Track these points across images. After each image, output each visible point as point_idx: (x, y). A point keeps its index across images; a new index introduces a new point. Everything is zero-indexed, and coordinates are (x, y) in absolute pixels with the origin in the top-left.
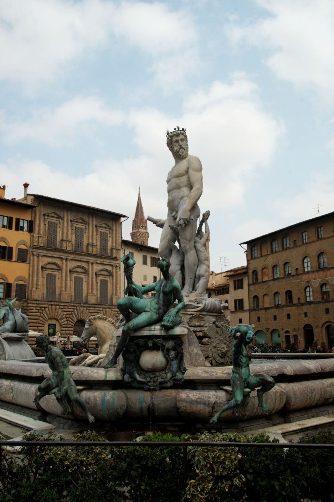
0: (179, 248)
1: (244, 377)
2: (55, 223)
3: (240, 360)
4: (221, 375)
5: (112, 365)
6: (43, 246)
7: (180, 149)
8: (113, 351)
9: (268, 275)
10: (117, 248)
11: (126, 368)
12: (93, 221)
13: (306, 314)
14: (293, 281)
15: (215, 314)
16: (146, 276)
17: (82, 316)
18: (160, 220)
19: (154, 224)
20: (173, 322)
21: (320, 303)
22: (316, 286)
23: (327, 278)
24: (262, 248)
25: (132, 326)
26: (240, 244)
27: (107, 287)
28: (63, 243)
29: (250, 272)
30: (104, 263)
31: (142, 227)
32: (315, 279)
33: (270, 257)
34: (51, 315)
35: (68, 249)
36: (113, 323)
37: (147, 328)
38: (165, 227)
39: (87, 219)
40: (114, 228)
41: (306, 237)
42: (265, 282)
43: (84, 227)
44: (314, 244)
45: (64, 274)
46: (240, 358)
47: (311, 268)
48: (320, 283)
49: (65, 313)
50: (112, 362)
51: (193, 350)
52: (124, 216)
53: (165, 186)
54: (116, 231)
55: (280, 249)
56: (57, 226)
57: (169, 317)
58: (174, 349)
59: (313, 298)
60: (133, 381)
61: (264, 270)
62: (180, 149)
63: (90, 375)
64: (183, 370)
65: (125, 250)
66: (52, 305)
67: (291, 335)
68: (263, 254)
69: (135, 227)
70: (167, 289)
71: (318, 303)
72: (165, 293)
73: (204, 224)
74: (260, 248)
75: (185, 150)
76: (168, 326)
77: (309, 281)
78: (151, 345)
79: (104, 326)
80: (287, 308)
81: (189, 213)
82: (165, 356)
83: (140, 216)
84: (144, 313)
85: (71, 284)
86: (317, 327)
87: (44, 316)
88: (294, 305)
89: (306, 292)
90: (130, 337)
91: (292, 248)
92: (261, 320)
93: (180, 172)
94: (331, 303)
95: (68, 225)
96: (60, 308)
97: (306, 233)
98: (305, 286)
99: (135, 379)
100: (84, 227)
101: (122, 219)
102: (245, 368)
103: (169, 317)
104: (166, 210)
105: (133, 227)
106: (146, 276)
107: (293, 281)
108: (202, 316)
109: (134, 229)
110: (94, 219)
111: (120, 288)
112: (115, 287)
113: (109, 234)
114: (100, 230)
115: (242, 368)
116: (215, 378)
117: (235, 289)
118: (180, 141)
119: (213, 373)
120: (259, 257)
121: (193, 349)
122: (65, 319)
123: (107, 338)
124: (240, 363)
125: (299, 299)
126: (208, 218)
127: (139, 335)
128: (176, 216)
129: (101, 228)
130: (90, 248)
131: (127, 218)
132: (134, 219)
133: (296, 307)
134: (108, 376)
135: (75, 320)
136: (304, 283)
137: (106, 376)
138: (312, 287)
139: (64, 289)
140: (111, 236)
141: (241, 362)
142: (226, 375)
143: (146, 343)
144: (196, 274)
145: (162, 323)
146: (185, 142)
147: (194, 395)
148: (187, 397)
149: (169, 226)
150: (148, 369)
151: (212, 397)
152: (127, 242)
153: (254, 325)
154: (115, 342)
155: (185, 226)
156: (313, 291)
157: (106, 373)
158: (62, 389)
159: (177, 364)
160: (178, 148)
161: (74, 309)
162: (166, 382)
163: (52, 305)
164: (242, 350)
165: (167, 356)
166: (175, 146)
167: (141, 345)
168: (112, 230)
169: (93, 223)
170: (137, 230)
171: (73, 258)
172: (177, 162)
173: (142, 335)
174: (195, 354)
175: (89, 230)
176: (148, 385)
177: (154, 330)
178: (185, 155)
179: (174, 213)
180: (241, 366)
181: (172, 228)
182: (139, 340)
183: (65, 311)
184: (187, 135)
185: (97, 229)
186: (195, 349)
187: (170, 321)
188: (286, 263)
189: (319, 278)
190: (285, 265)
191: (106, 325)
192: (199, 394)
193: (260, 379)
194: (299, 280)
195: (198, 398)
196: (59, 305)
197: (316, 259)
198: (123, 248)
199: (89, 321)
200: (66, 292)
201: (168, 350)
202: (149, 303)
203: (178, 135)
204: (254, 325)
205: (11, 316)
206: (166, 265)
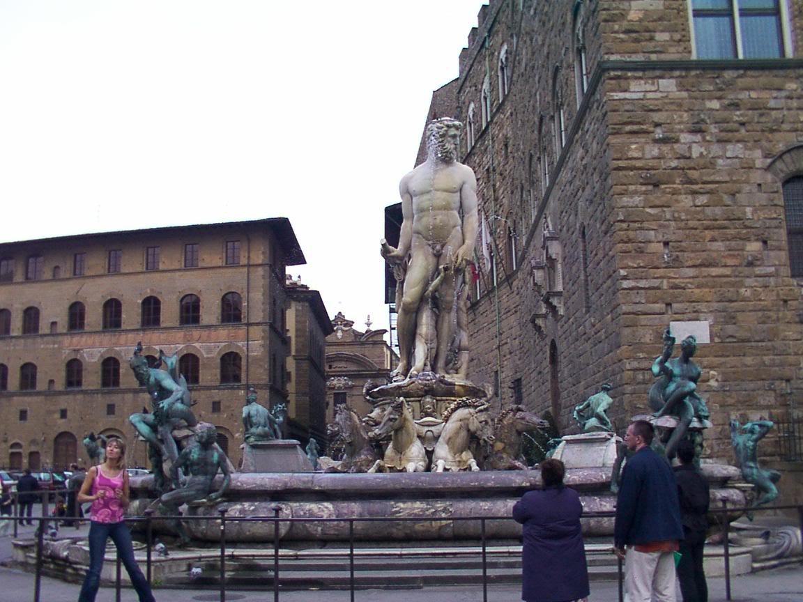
13: (64, 414)
14: (42, 346)
21: (97, 394)
22: (93, 361)
23: (117, 349)
32: (92, 347)
44: (99, 281)
48: (102, 356)
55: (19, 277)
67: (25, 451)
71: (94, 394)
77: (78, 350)
80: (21, 398)
88: (39, 394)
91: (46, 281)
94: (120, 396)
107: (42, 346)
125: (51, 382)
133: (43, 397)
136: (67, 351)
166: (449, 142)
189: (101, 346)
193: (772, 474)
194: (56, 346)
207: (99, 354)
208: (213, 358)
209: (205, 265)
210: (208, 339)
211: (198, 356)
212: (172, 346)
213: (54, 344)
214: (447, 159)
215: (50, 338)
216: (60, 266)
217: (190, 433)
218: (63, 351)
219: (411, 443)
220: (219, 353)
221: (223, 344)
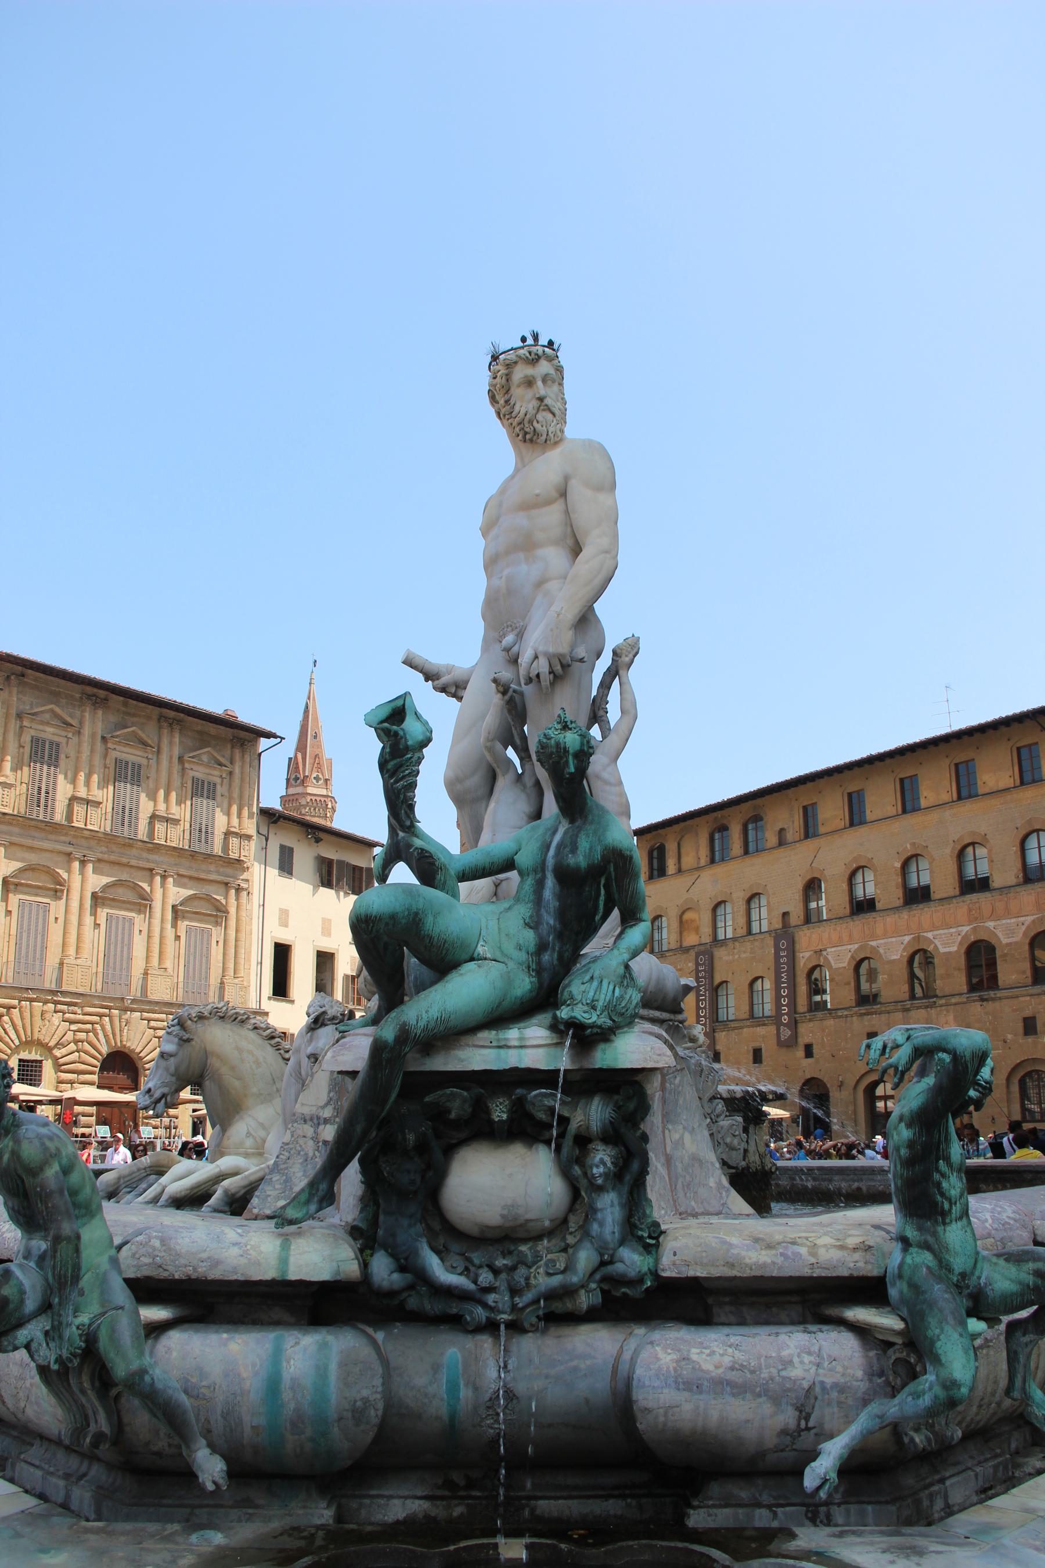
0: (520, 771)
1: (959, 1263)
2: (51, 743)
3: (938, 1185)
4: (835, 1255)
5: (313, 1207)
6: (11, 812)
8: (311, 1143)
10: (243, 832)
11: (374, 1223)
12: (171, 743)
15: (657, 1014)
16: (330, 920)
17: (125, 1039)
18: (450, 669)
19: (427, 680)
20: (610, 1008)
23: (873, 943)
24: (683, 851)
25: (421, 1024)
27: (209, 949)
28: (76, 808)
30: (203, 876)
31: (317, 779)
33: (706, 875)
34: (29, 1034)
35: (89, 827)
36: (273, 1038)
37: (486, 1036)
38: (467, 694)
39: (151, 739)
40: (237, 770)
42: (686, 950)
43: (144, 762)
45: (75, 904)
46: (936, 1176)
48: (852, 957)
49: (74, 1027)
50: (311, 1196)
51: (679, 1143)
52: (269, 735)
53: (476, 547)
54: (242, 780)
56: (57, 752)
57: (595, 983)
58: (611, 1136)
60: (411, 1287)
61: (688, 916)
63: (204, 1255)
64: (646, 1235)
65: (267, 840)
66: (31, 1000)
68: (684, 867)
69: (297, 779)
70: (580, 859)
72: (566, 876)
73: (616, 682)
74: (676, 851)
76: (593, 1026)
78: (505, 1116)
79: (237, 1048)
81: (571, 633)
82: (565, 1172)
83: (312, 747)
85: (94, 940)
86: (840, 1086)
87: (6, 1033)
90: (407, 1074)
93: (537, 491)
95: (92, 751)
96: (55, 1012)
98: (810, 965)
99: (422, 1278)
100: (144, 762)
101: (264, 743)
102: (959, 1223)
103: (595, 983)
104: (477, 629)
105: (288, 780)
106: (330, 920)
109: (292, 786)
110: (177, 740)
111: (249, 954)
112: (231, 951)
113: (218, 787)
114: (192, 773)
115: (944, 1223)
116: (806, 1272)
119: (796, 1248)
121: (682, 1138)
122: (72, 1047)
123: (246, 1095)
124: (939, 1198)
126: (632, 662)
127: (451, 1067)
128: (515, 649)
129: (195, 767)
130: (160, 828)
131: (279, 740)
132: (292, 755)
134: (292, 1260)
135: (105, 1050)
136: (807, 955)
137: (284, 1261)
139: (72, 951)
140: (227, 794)
141: (943, 1195)
142: (857, 1256)
143: (480, 1107)
145: (564, 1013)
146: (555, 388)
147: (712, 1353)
148: (677, 1361)
149: (495, 681)
150: (485, 1228)
151: (796, 1360)
152: (274, 815)
154: (322, 1104)
155: (552, 684)
157: (286, 1246)
158: (69, 1325)
159: (622, 1206)
160: (531, 406)
161: (101, 1016)
162: (568, 1292)
163: (31, 1000)
164: (947, 1140)
165: (577, 1170)
167: (453, 1115)
168: (231, 773)
169: (171, 750)
170: (299, 790)
171: (106, 857)
172: (522, 463)
173: (459, 1067)
174: (686, 1160)
175: (158, 770)
176: (485, 1305)
177: (521, 1047)
179: (510, 638)
180: (944, 1214)
181: (504, 689)
182: (448, 1091)
183: (72, 1022)
184: (562, 363)
185: (183, 769)
186: (687, 1137)
187: (600, 1005)
189: (851, 942)
190: (749, 901)
191: (244, 1044)
192: (737, 1347)
195: (732, 1368)
196: (56, 1003)
197: (845, 886)
198: (264, 831)
199: (179, 1024)
200: (79, 962)
201: (583, 1141)
202: (493, 924)
206: (577, 747)
207: (850, 954)
208: (1016, 943)
209: (987, 790)
210: (1008, 913)
211: (993, 942)
212: (953, 930)
216: (785, 826)
218: (801, 955)
219: (238, 1113)
220: (1025, 934)
221: (1030, 919)
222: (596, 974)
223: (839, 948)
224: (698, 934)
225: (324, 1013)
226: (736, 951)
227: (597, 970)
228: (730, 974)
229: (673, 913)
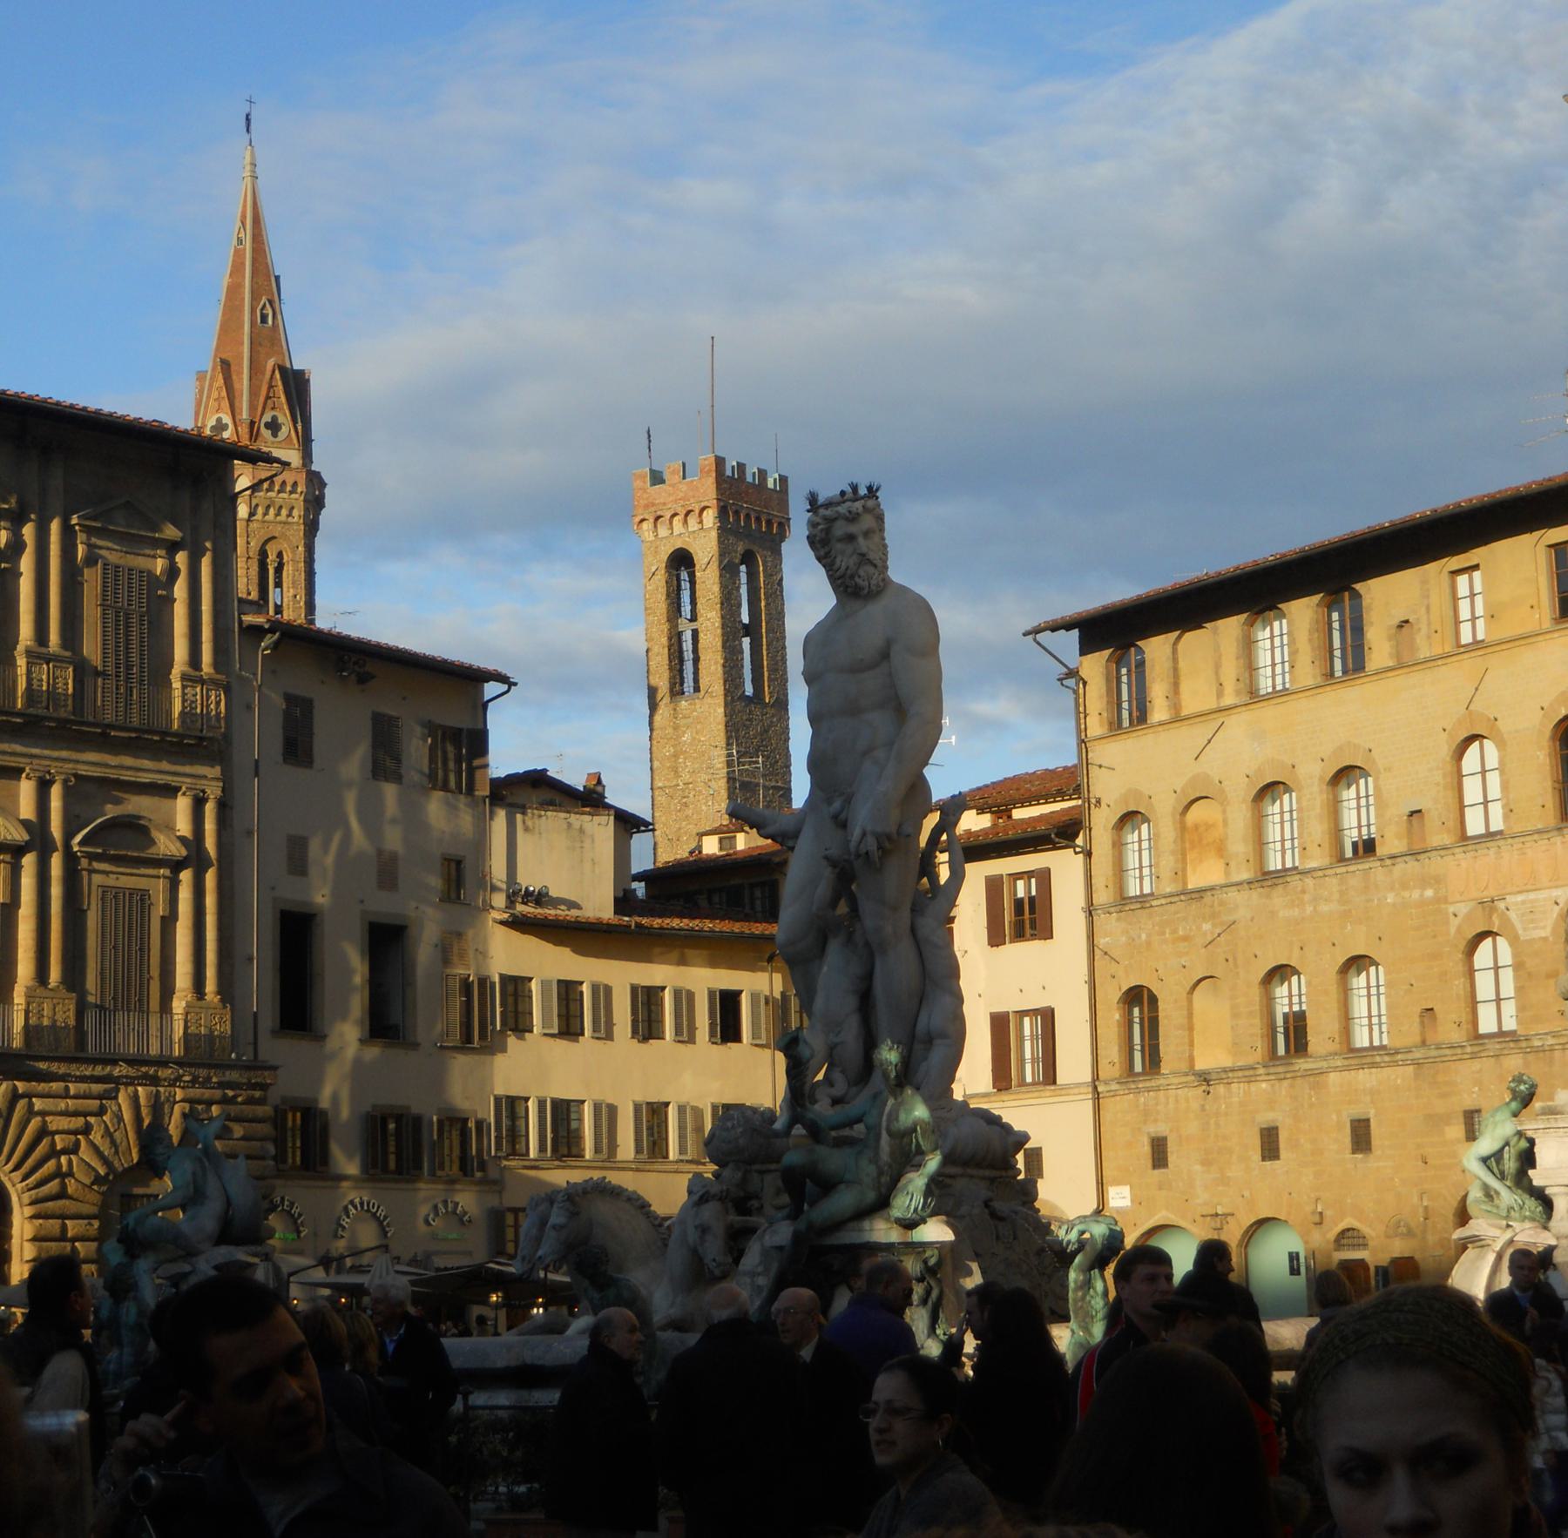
7: (859, 565)
9: (1220, 849)
26: (1037, 631)
29: (1101, 822)
33: (1238, 726)
41: (1479, 600)
42: (1200, 892)
47: (1509, 812)
59: (1521, 1009)
62: (859, 565)
75: (875, 566)
84: (842, 1186)
89: (1471, 972)
92: (1172, 1159)
97: (1477, 575)
98: (1471, 933)
103: (910, 1197)
108: (948, 1181)
117: (996, 938)
118: (861, 540)
120: (1161, 724)
128: (843, 816)
136: (1462, 909)
138: (1514, 941)
144: (915, 1025)
153: (1125, 1190)
155: (880, 858)
156: (1518, 966)
178: (878, 585)
179: (837, 805)
188: (1345, 775)
194: (1429, 893)
199: (568, 1199)
203: (853, 518)
204: (1125, 1190)
205: (212, 1188)
213: (1423, 888)
214: (849, 590)
215: (1411, 866)
217: (187, 1268)
218: (1451, 909)
222: (910, 1191)
223: (1532, 896)
224: (1222, 857)
225: (707, 1192)
226: (1307, 897)
227: (911, 1188)
228: (1296, 950)
229: (1163, 808)
